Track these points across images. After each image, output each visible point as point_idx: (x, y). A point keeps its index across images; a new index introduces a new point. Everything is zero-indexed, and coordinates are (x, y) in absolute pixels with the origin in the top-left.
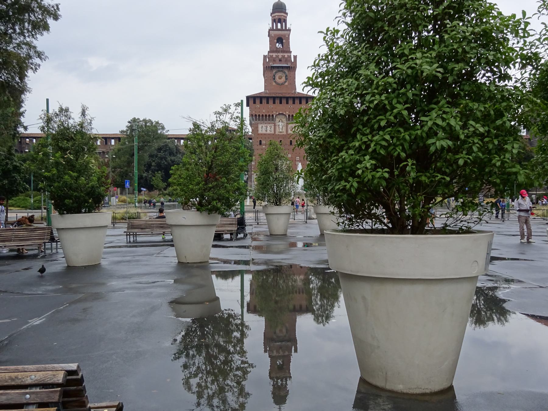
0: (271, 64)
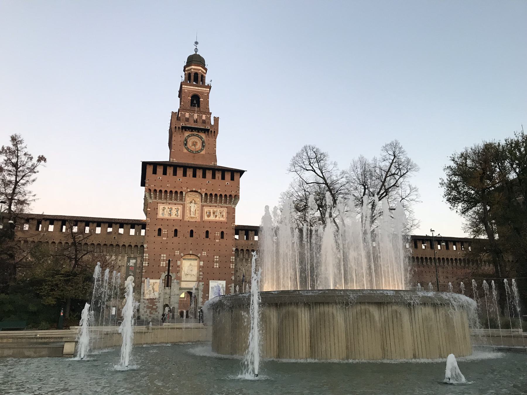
0: (182, 124)
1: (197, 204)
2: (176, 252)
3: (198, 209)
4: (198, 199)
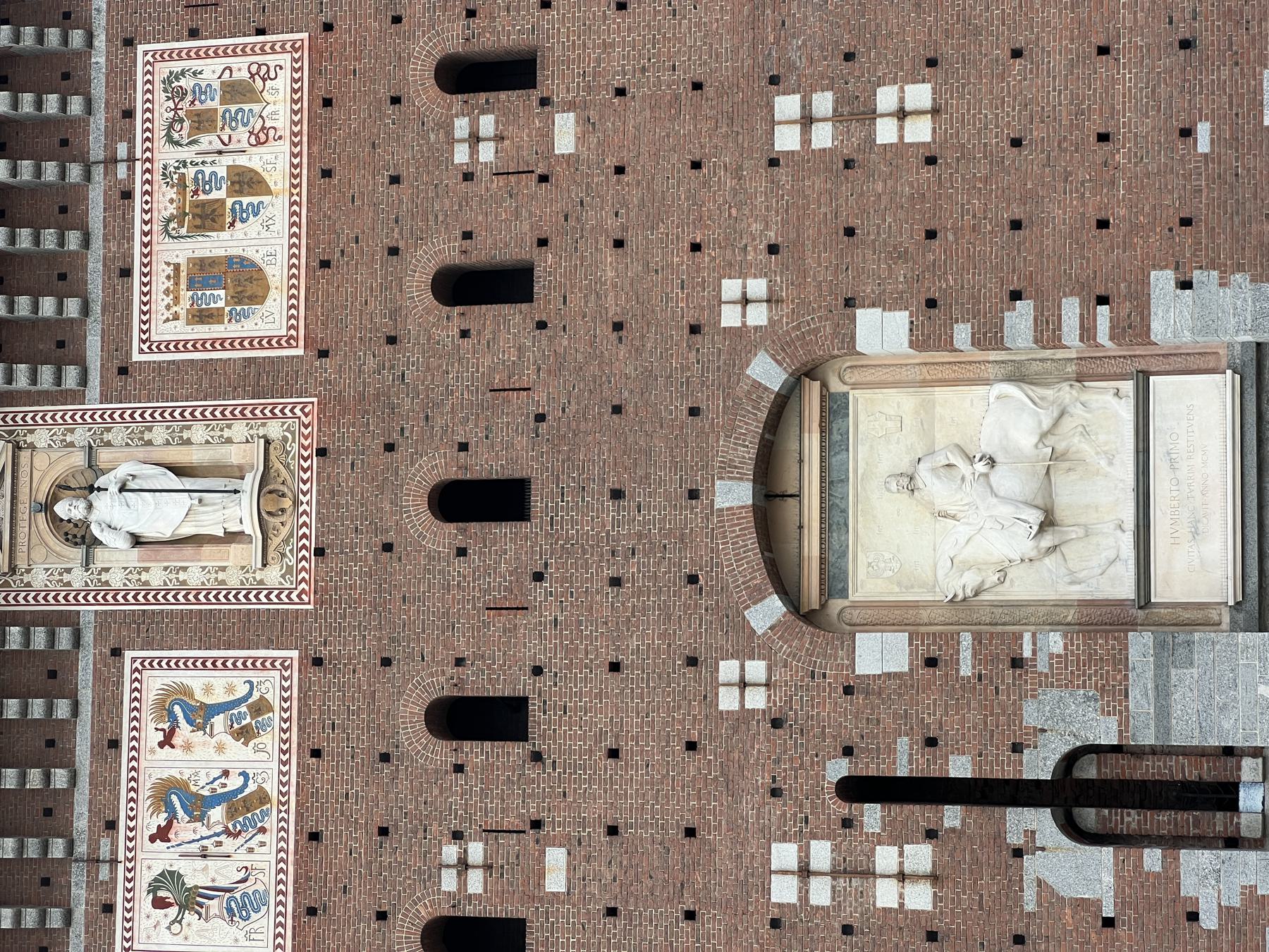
1: (104, 456)
2: (728, 701)
3: (159, 434)
4: (41, 437)
